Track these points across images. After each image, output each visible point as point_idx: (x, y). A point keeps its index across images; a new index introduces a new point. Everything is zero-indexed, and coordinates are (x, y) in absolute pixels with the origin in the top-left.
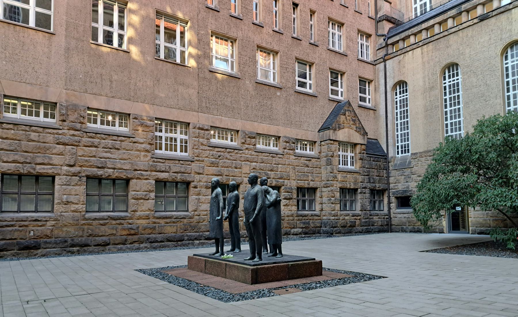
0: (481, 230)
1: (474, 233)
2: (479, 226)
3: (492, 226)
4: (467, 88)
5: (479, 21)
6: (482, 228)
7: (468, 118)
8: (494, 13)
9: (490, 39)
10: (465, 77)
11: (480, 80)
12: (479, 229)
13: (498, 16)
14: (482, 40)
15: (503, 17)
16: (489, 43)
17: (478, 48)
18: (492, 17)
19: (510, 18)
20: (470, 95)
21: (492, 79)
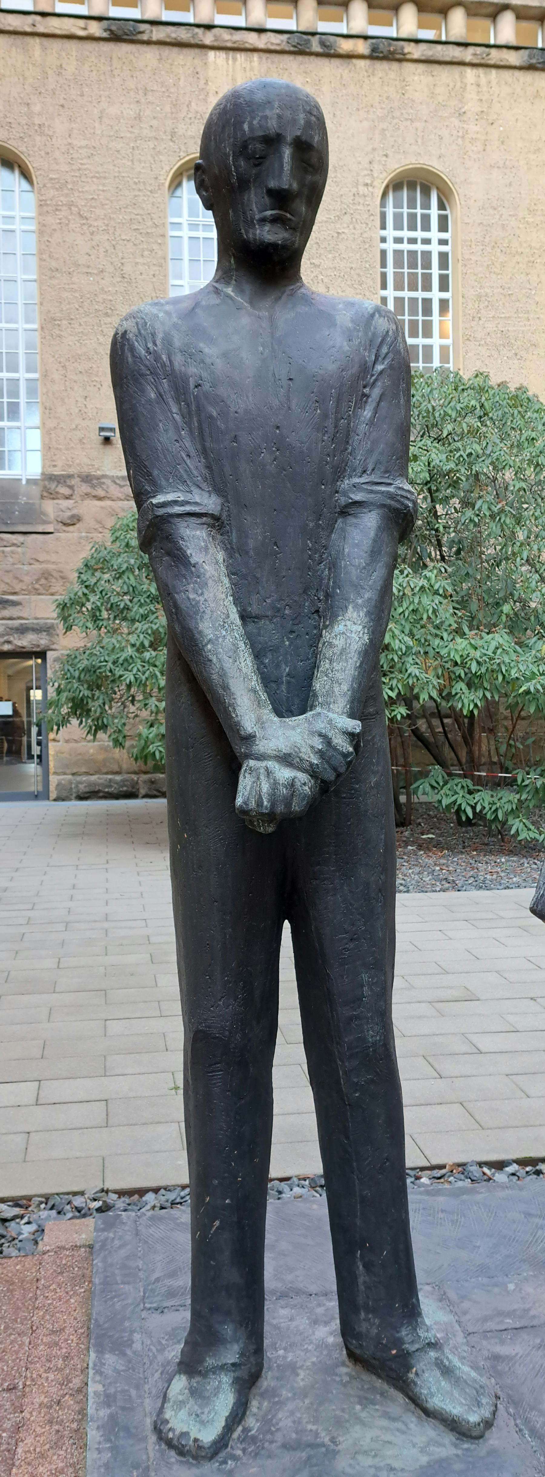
0: (90, 784)
1: (64, 794)
2: (83, 769)
3: (125, 767)
4: (54, 264)
5: (105, 35)
6: (93, 778)
7: (56, 376)
8: (158, 33)
9: (139, 118)
10: (50, 220)
11: (102, 250)
12: (86, 781)
13: (166, 51)
14: (113, 110)
15: (183, 59)
16: (136, 131)
17: (98, 132)
18: (149, 43)
19: (201, 76)
20: (65, 295)
21: (140, 260)
